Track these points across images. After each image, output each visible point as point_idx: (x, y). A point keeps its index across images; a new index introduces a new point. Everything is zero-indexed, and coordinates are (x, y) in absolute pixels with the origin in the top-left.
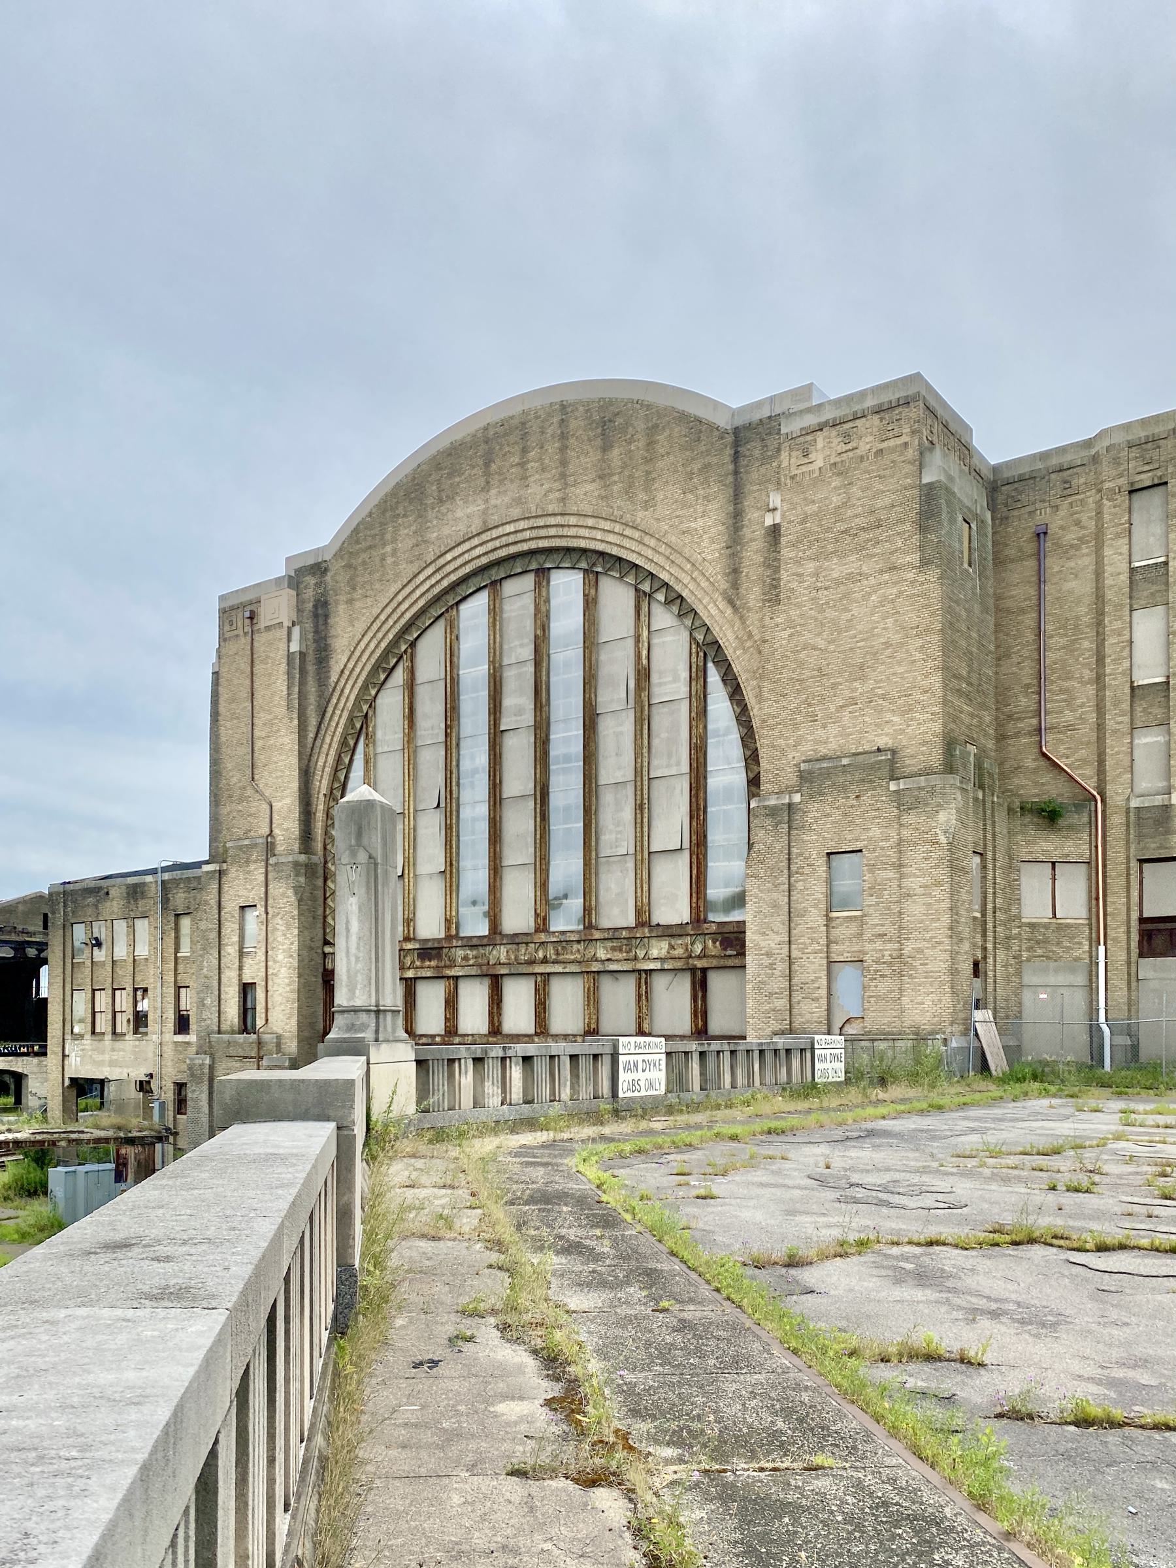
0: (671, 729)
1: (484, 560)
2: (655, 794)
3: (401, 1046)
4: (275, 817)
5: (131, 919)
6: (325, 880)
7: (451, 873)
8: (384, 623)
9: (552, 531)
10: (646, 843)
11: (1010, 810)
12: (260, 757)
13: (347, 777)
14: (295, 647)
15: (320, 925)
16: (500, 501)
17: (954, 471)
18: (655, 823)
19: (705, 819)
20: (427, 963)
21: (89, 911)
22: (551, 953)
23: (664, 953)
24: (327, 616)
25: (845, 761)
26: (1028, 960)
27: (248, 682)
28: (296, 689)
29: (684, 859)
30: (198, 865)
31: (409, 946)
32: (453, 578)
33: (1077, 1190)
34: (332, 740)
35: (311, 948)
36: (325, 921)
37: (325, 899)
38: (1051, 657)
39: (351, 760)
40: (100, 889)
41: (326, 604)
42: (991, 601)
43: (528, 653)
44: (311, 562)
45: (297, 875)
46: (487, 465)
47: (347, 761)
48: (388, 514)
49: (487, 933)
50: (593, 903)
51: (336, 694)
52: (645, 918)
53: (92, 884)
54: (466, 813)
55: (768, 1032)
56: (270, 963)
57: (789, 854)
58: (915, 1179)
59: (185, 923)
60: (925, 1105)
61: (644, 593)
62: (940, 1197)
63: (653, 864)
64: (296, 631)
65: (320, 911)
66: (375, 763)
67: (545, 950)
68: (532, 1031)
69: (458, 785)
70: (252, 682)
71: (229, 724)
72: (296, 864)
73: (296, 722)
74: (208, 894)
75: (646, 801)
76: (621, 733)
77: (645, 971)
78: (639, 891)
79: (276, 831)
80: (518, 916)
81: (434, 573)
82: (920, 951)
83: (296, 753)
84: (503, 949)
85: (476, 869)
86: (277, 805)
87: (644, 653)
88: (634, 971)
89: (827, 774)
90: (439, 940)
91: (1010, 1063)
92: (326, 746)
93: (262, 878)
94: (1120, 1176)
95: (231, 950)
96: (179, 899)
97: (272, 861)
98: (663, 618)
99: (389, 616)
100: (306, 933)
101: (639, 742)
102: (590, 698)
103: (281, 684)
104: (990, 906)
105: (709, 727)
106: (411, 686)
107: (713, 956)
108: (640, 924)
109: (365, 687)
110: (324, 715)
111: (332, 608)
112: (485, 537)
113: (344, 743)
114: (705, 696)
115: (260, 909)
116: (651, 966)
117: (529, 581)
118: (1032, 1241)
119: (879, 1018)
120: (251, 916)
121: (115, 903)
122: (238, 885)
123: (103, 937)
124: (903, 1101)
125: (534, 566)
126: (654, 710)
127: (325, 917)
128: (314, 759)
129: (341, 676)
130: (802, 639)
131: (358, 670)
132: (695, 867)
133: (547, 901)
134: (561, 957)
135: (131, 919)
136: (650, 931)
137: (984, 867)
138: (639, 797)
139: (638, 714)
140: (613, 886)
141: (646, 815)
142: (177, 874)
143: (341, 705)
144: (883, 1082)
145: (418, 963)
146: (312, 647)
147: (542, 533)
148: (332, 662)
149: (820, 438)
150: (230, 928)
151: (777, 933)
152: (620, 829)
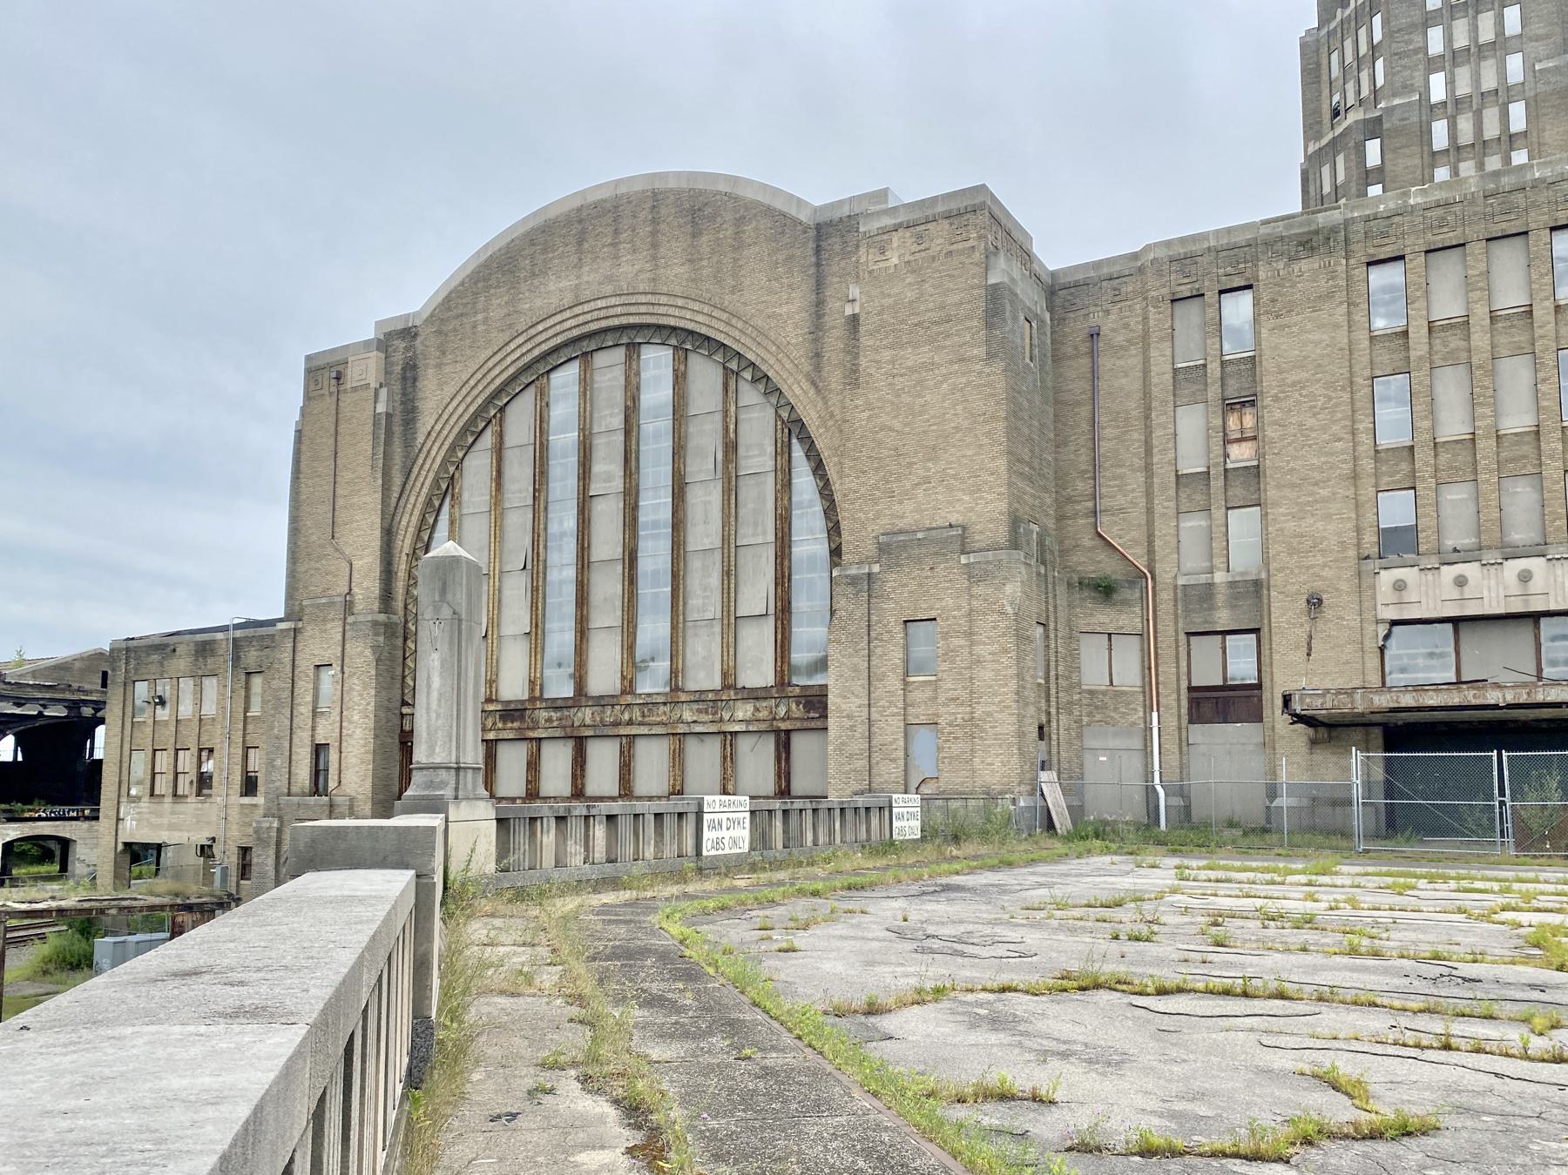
0: (759, 499)
1: (575, 332)
2: (741, 562)
3: (482, 804)
4: (355, 575)
5: (198, 677)
6: (405, 639)
7: (536, 635)
9: (643, 309)
11: (1070, 585)
12: (342, 516)
13: (430, 537)
14: (381, 408)
16: (591, 277)
17: (1016, 274)
21: (154, 668)
24: (415, 380)
26: (1089, 725)
29: (769, 626)
30: (271, 623)
31: (491, 707)
33: (1138, 939)
35: (388, 709)
38: (1105, 447)
39: (436, 520)
40: (167, 645)
42: (1051, 393)
43: (618, 421)
44: (400, 326)
45: (376, 634)
48: (480, 285)
51: (422, 456)
53: (157, 642)
54: (553, 576)
55: (848, 792)
58: (988, 930)
59: (257, 682)
60: (996, 861)
62: (1011, 947)
64: (384, 392)
69: (546, 547)
71: (310, 483)
72: (375, 623)
79: (355, 590)
80: (604, 677)
82: (989, 714)
84: (588, 711)
85: (562, 630)
86: (357, 564)
87: (732, 427)
90: (522, 702)
91: (1074, 823)
92: (410, 506)
94: (1177, 926)
95: (304, 710)
96: (251, 657)
97: (350, 619)
98: (750, 395)
103: (366, 446)
104: (1052, 673)
105: (794, 499)
106: (499, 450)
108: (726, 687)
111: (420, 372)
112: (577, 310)
113: (429, 502)
116: (737, 728)
117: (619, 354)
118: (1097, 986)
119: (952, 779)
120: (327, 676)
121: (182, 661)
123: (167, 696)
124: (975, 857)
125: (625, 340)
126: (741, 482)
127: (404, 677)
130: (878, 421)
131: (445, 432)
133: (634, 663)
135: (198, 677)
137: (1047, 637)
142: (250, 632)
143: (427, 466)
144: (956, 839)
146: (399, 408)
147: (633, 309)
149: (896, 239)
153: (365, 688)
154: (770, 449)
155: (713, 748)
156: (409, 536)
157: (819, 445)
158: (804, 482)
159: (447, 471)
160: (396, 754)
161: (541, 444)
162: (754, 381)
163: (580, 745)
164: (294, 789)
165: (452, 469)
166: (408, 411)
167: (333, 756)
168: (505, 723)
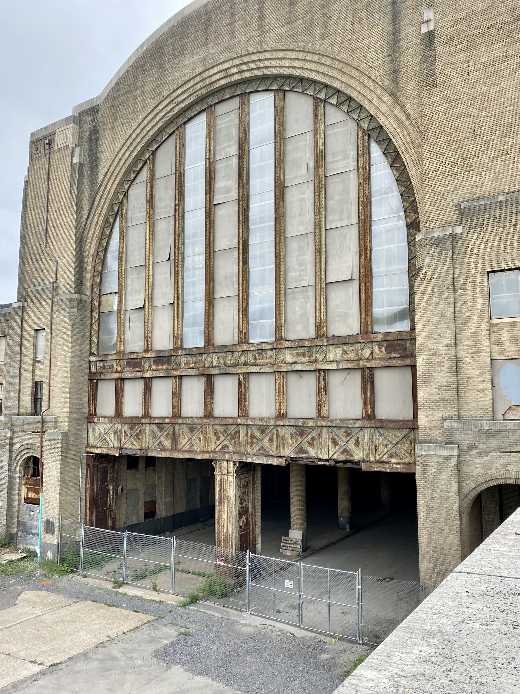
2: (329, 241)
4: (60, 270)
6: (92, 312)
7: (178, 305)
8: (134, 140)
9: (252, 66)
10: (323, 277)
13: (108, 243)
14: (76, 160)
15: (88, 342)
18: (331, 261)
19: (371, 256)
20: (160, 367)
22: (250, 358)
23: (338, 357)
24: (97, 140)
25: (501, 198)
27: (46, 185)
28: (76, 186)
30: (9, 305)
31: (148, 355)
32: (182, 106)
34: (98, 219)
36: (91, 339)
37: (91, 325)
39: (111, 232)
41: (97, 132)
43: (234, 150)
45: (71, 308)
46: (206, 28)
47: (108, 233)
49: (203, 345)
50: (283, 322)
54: (189, 262)
56: (52, 368)
57: (453, 274)
61: (321, 100)
63: (329, 293)
64: (77, 151)
65: (88, 333)
66: (126, 233)
67: (246, 357)
68: (236, 415)
69: (183, 244)
70: (48, 185)
71: (33, 213)
72: (71, 300)
73: (75, 207)
74: (15, 322)
75: (323, 246)
76: (304, 199)
77: (324, 370)
78: (318, 311)
79: (60, 279)
80: (226, 333)
81: (169, 103)
83: (74, 228)
84: (215, 357)
85: (196, 300)
86: (61, 262)
87: (321, 141)
88: (315, 370)
89: (486, 209)
90: (169, 351)
93: (49, 310)
95: (28, 359)
99: (138, 135)
100: (77, 347)
101: (318, 204)
102: (280, 176)
103: (66, 185)
105: (373, 189)
106: (152, 181)
107: (380, 359)
108: (319, 336)
109: (121, 184)
110: (93, 202)
111: (101, 134)
113: (106, 221)
114: (369, 167)
115: (48, 330)
116: (329, 367)
122: (34, 316)
126: (329, 180)
127: (91, 337)
128: (86, 232)
129: (105, 176)
131: (116, 172)
132: (363, 292)
134: (257, 362)
136: (327, 341)
138: (317, 244)
139: (317, 185)
140: (297, 309)
141: (323, 256)
143: (105, 196)
145: (154, 367)
146: (88, 159)
148: (100, 168)
150: (28, 343)
151: (444, 337)
152: (303, 268)
153: (65, 344)
154: (353, 154)
155: (309, 383)
156: (94, 243)
157: (397, 142)
158: (382, 173)
159: (118, 199)
160: (86, 387)
161: (180, 173)
162: (339, 105)
163: (210, 381)
164: (22, 411)
165: (121, 197)
166: (93, 160)
167: (45, 389)
168: (157, 366)
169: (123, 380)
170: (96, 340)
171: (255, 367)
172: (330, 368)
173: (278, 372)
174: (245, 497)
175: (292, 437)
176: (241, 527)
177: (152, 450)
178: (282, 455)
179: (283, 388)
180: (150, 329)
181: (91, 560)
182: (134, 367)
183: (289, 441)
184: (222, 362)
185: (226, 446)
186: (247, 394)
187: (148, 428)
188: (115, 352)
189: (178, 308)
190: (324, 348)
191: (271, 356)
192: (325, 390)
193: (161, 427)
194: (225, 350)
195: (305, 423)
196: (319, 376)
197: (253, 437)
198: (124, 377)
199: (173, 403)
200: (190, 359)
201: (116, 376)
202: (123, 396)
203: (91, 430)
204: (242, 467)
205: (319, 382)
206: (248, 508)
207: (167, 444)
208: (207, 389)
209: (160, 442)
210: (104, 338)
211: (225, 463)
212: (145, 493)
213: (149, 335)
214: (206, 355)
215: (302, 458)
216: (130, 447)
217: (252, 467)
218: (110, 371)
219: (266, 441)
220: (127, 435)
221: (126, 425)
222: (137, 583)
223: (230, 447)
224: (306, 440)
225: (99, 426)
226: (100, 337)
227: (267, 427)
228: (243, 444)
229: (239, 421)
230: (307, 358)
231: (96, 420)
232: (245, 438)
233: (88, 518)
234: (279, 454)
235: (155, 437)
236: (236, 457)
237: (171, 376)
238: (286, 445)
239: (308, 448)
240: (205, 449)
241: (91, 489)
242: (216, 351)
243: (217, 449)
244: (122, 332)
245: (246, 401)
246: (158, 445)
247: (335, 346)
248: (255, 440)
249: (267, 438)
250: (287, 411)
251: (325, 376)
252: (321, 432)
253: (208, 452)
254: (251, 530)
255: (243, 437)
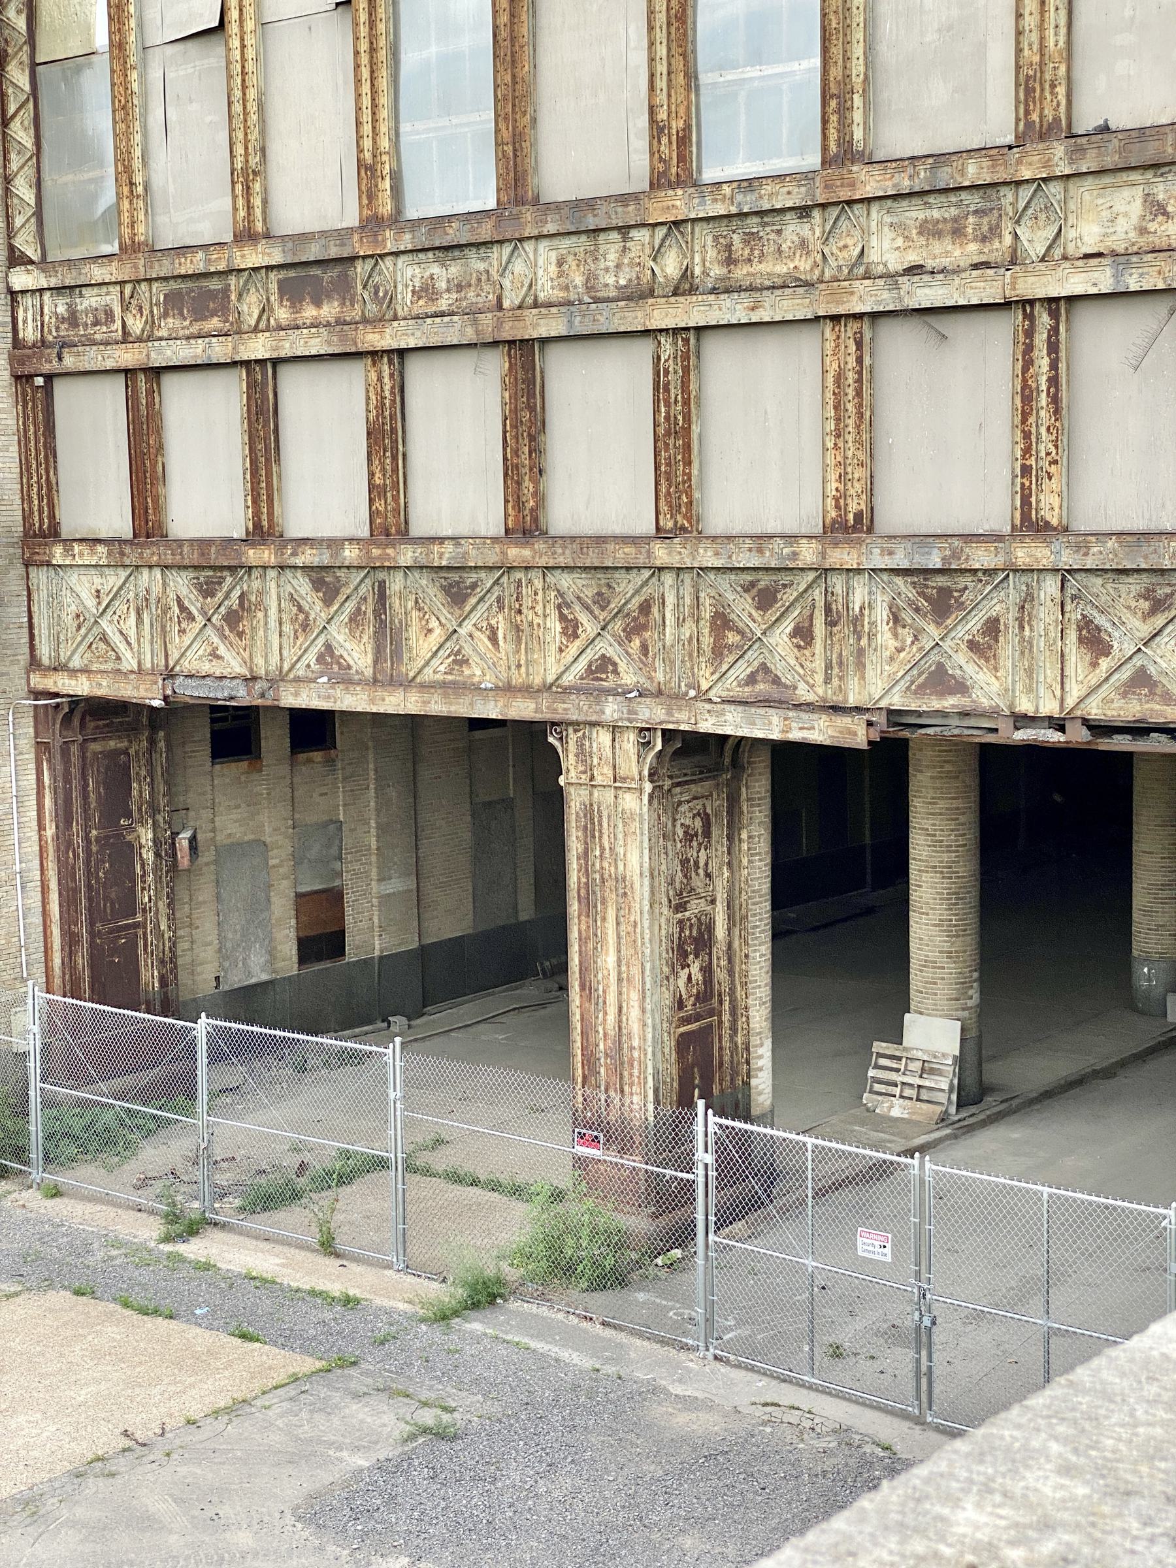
20: (309, 312)
22: (705, 258)
23: (1123, 234)
31: (252, 257)
49: (491, 204)
50: (857, 68)
52: (1050, 108)
67: (687, 250)
77: (1052, 303)
88: (1006, 305)
108: (1033, 132)
116: (1076, 283)
134: (740, 272)
136: (1076, 152)
145: (282, 314)
169: (156, 373)
170: (29, 196)
171: (726, 301)
172: (1079, 290)
173: (835, 318)
174: (698, 882)
175: (896, 619)
176: (681, 1004)
177: (297, 680)
178: (852, 701)
179: (859, 393)
180: (254, 136)
181: (77, 1125)
182: (200, 315)
183: (885, 637)
184: (579, 280)
185: (605, 665)
186: (695, 429)
187: (272, 586)
188: (114, 248)
189: (372, 24)
190: (1054, 189)
191: (803, 244)
192: (1055, 400)
193: (325, 580)
194: (591, 222)
195: (956, 555)
196: (1030, 333)
197: (722, 622)
198: (157, 361)
199: (371, 475)
200: (435, 269)
201: (128, 357)
202: (161, 447)
203: (41, 597)
204: (677, 753)
205: (1028, 363)
206: (711, 928)
207: (358, 654)
208: (514, 411)
209: (329, 647)
210: (57, 180)
211: (603, 738)
212: (298, 859)
213: (254, 160)
214: (507, 249)
215: (943, 714)
216: (206, 667)
217: (728, 752)
218: (100, 333)
219: (781, 638)
220: (192, 618)
221: (184, 574)
222: (260, 1222)
223: (622, 666)
224: (960, 632)
225: (73, 578)
226: (47, 183)
227: (785, 578)
228: (679, 654)
229: (662, 554)
230: (973, 247)
231: (58, 554)
232: (688, 630)
233: (57, 961)
234: (837, 699)
235: (305, 626)
236: (653, 713)
237: (358, 355)
238: (871, 658)
239: (970, 669)
240: (518, 678)
241: (64, 843)
242: (551, 228)
243: (569, 679)
244: (138, 153)
245: (688, 463)
246: (320, 659)
247: (1108, 180)
248: (732, 638)
249: (788, 626)
250: (878, 500)
251: (1054, 330)
252: (1030, 597)
253: (527, 690)
254: (726, 1017)
255: (680, 623)
